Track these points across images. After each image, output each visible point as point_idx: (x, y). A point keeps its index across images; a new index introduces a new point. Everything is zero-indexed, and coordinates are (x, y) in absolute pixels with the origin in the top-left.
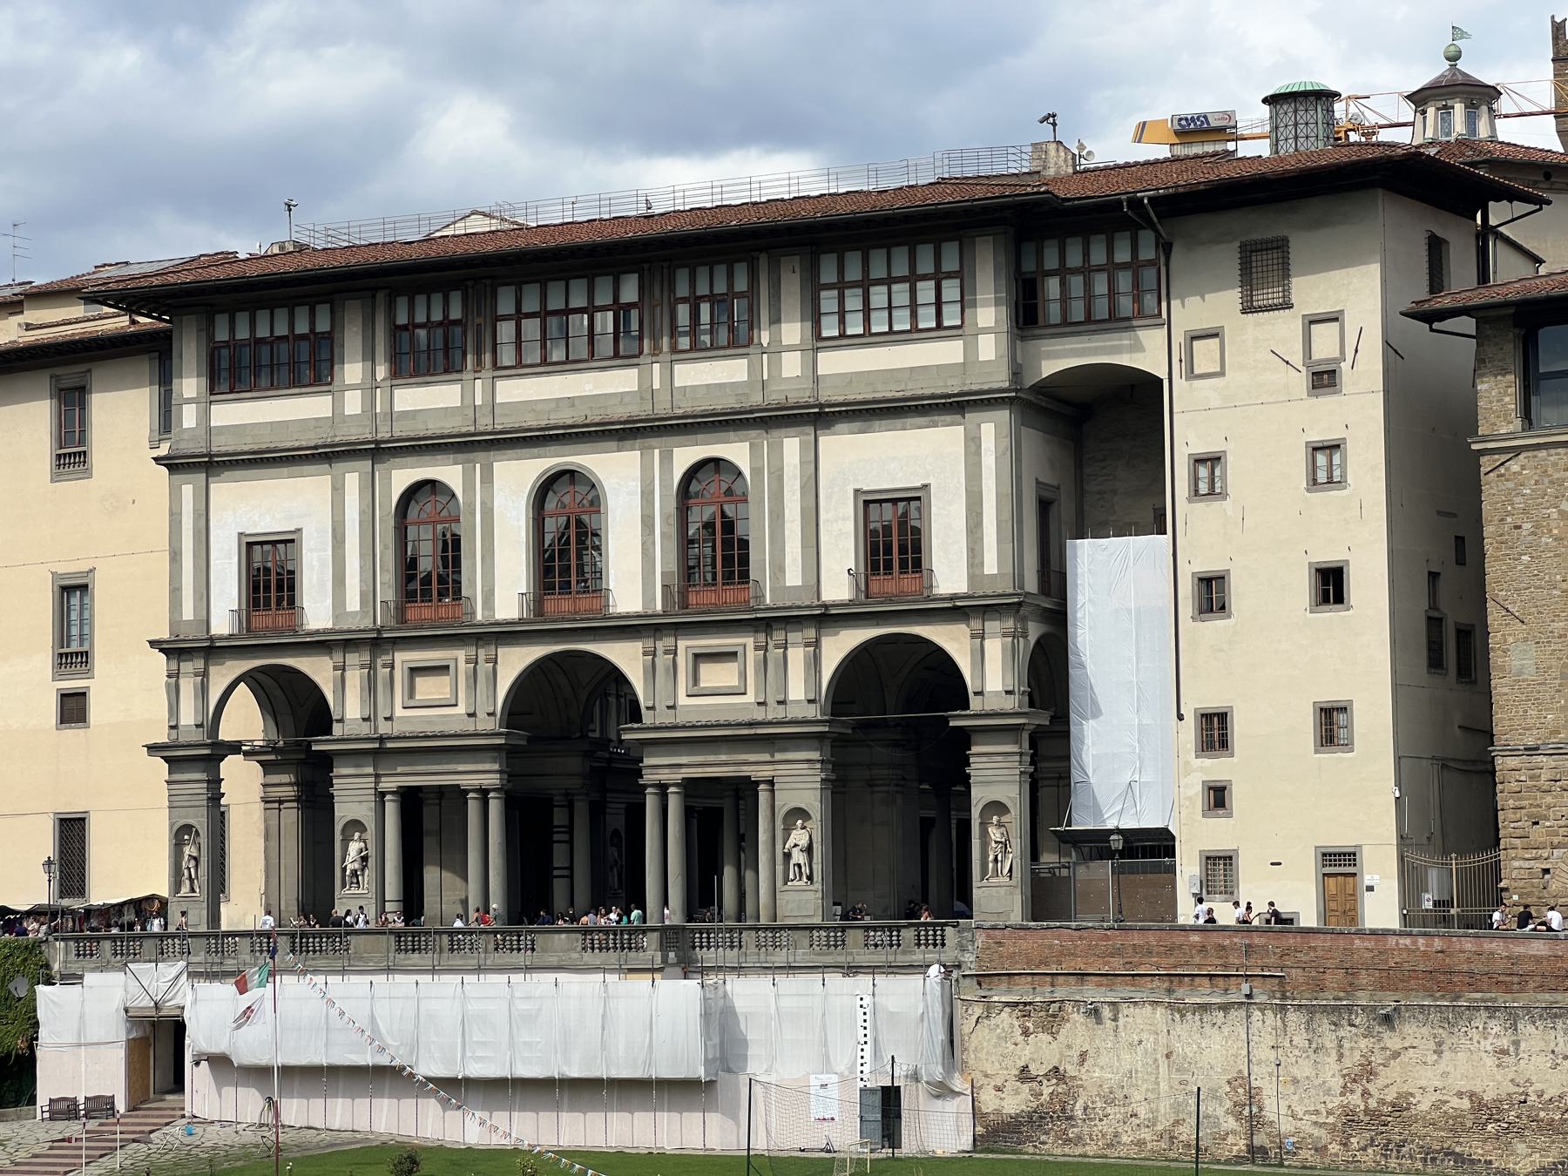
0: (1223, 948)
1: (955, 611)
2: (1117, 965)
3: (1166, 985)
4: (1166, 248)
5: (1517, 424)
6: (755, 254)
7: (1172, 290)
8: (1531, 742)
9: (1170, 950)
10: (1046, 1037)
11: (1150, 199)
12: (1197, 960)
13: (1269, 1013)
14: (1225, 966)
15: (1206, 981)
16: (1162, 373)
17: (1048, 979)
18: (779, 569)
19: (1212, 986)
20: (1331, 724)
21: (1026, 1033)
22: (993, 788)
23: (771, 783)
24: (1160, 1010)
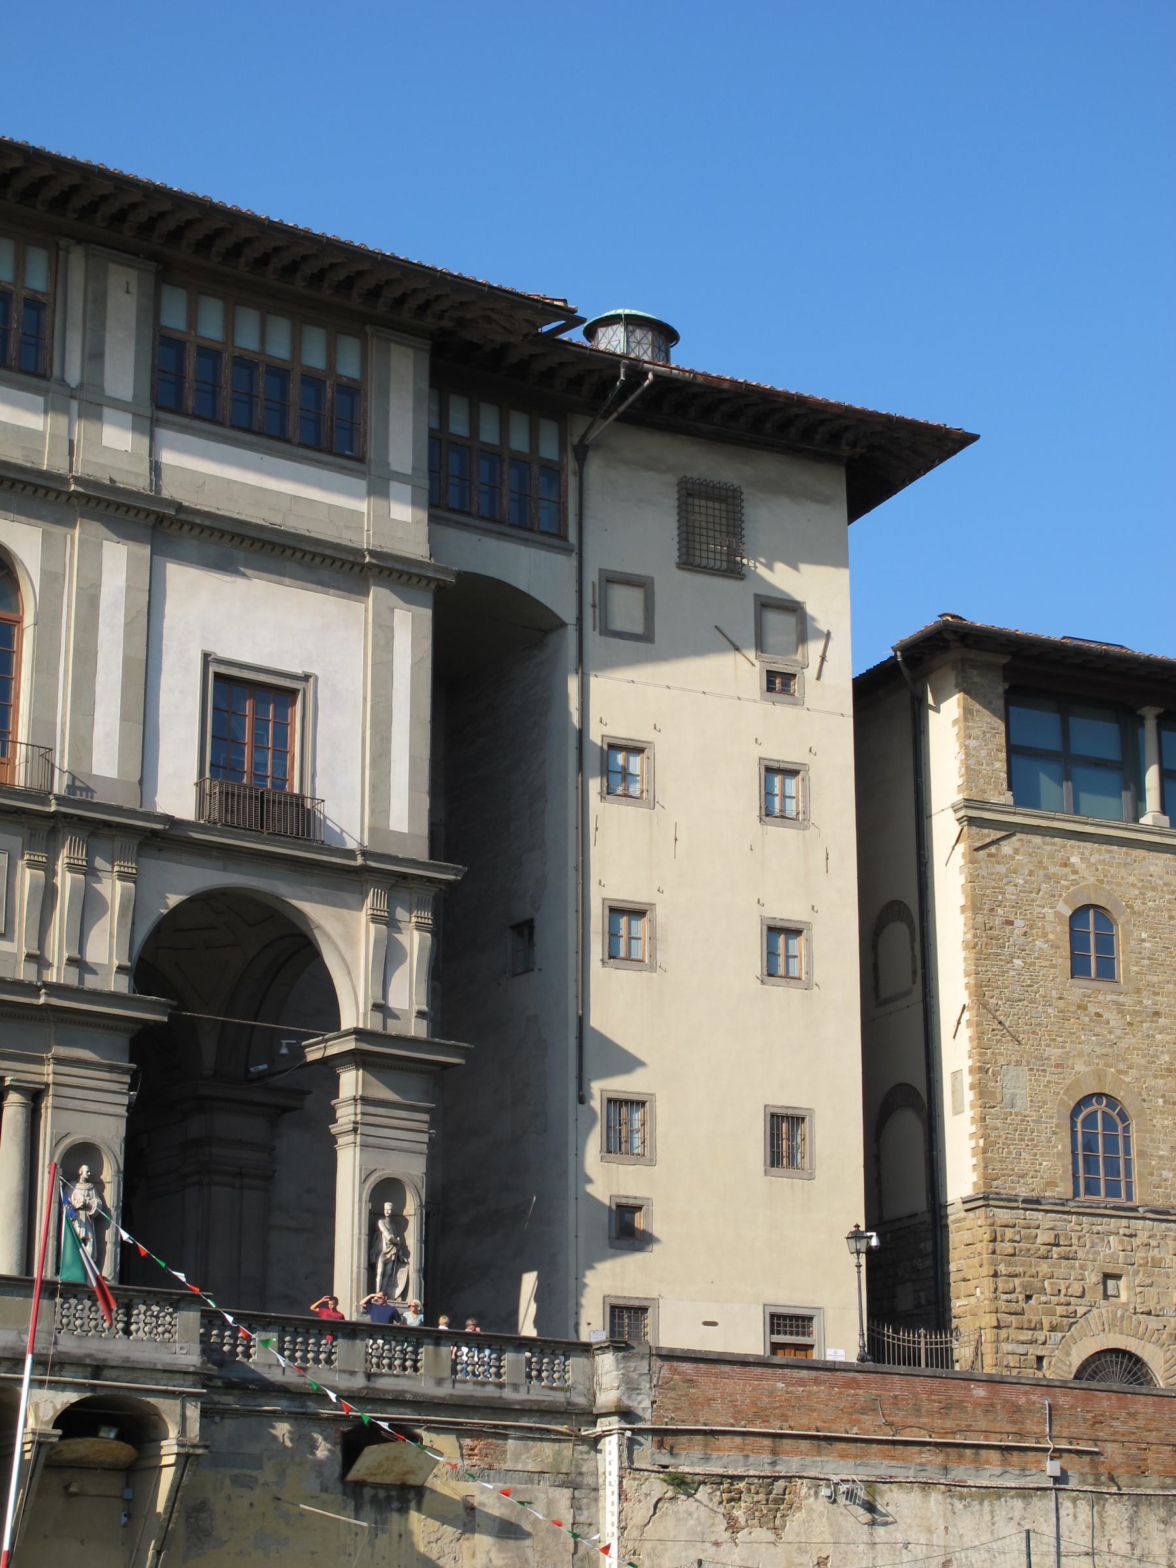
0: (1017, 1409)
1: (349, 876)
2: (870, 1426)
3: (940, 1459)
4: (582, 453)
5: (1008, 798)
6: (63, 242)
7: (589, 513)
8: (1023, 1192)
9: (946, 1409)
10: (765, 1534)
11: (656, 375)
12: (982, 1424)
13: (1083, 1507)
14: (1021, 1435)
15: (994, 1456)
16: (568, 614)
17: (767, 1442)
18: (82, 743)
19: (1005, 1463)
20: (784, 1136)
21: (733, 1526)
22: (394, 1157)
23: (34, 1097)
24: (935, 1498)
